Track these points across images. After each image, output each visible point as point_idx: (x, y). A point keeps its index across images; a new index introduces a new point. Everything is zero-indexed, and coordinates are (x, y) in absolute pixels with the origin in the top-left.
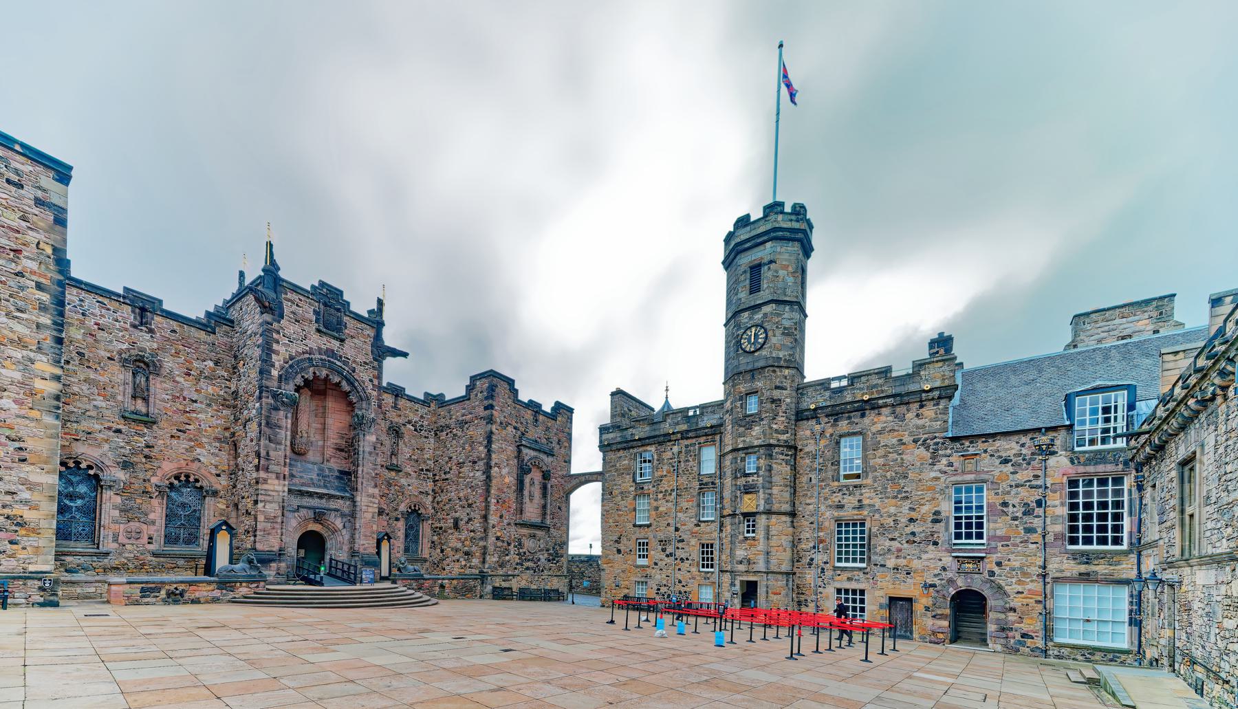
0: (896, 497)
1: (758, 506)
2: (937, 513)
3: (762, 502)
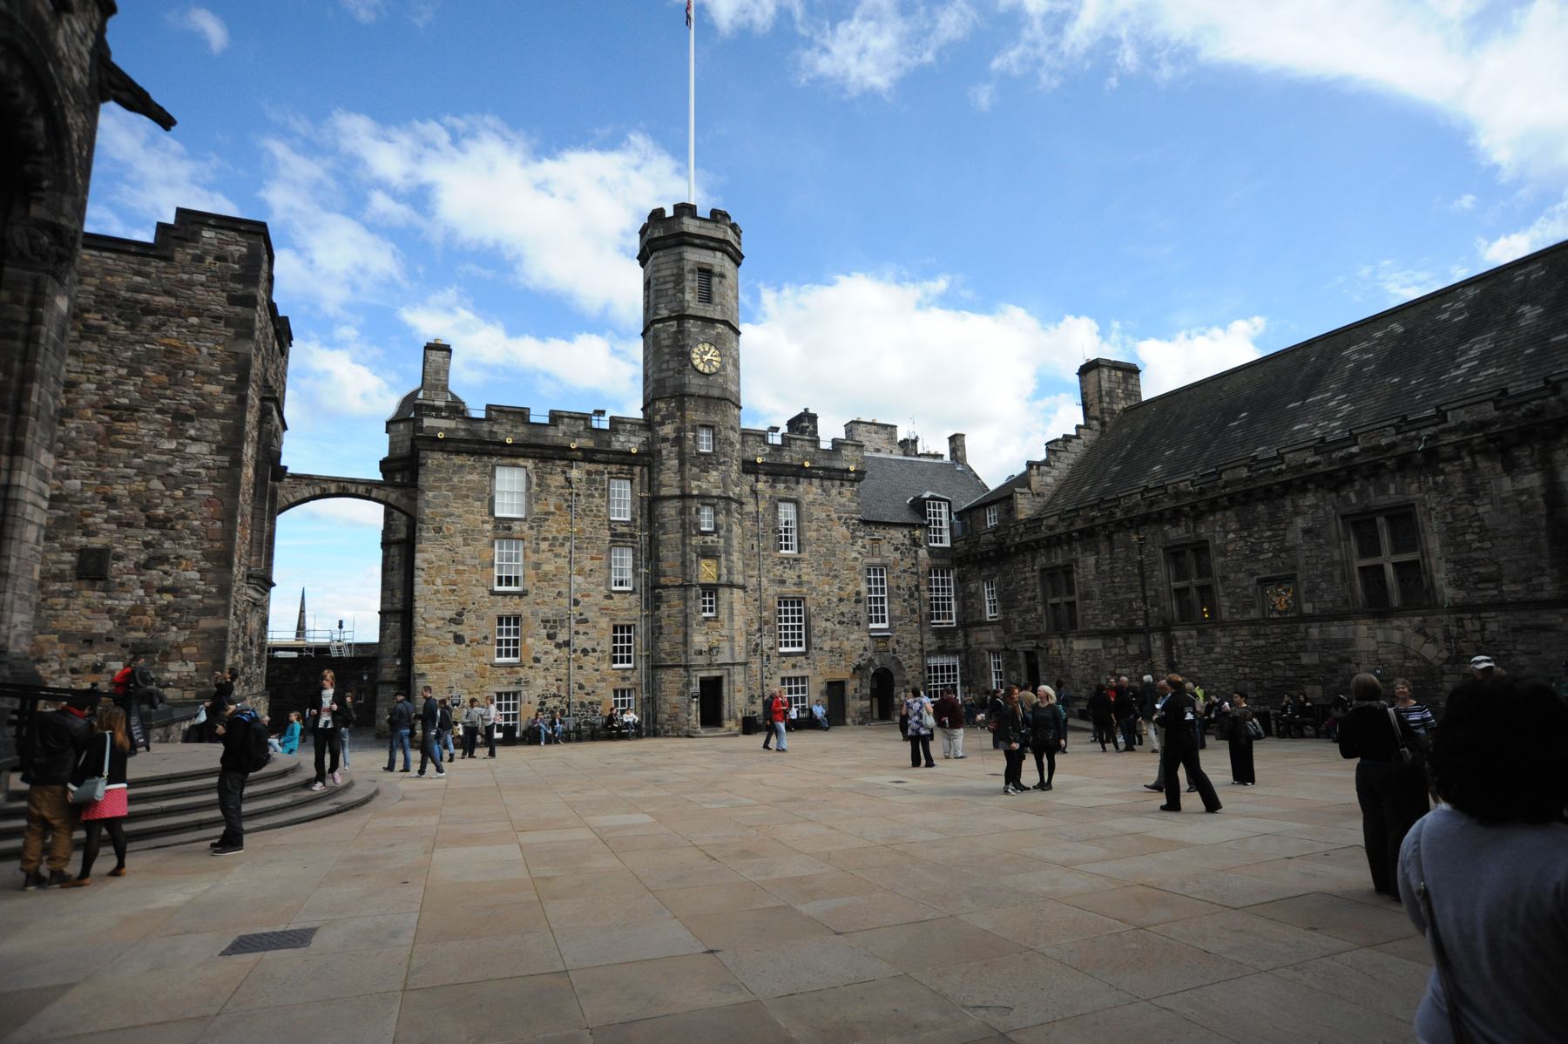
1: (719, 576)
2: (858, 593)
3: (724, 571)
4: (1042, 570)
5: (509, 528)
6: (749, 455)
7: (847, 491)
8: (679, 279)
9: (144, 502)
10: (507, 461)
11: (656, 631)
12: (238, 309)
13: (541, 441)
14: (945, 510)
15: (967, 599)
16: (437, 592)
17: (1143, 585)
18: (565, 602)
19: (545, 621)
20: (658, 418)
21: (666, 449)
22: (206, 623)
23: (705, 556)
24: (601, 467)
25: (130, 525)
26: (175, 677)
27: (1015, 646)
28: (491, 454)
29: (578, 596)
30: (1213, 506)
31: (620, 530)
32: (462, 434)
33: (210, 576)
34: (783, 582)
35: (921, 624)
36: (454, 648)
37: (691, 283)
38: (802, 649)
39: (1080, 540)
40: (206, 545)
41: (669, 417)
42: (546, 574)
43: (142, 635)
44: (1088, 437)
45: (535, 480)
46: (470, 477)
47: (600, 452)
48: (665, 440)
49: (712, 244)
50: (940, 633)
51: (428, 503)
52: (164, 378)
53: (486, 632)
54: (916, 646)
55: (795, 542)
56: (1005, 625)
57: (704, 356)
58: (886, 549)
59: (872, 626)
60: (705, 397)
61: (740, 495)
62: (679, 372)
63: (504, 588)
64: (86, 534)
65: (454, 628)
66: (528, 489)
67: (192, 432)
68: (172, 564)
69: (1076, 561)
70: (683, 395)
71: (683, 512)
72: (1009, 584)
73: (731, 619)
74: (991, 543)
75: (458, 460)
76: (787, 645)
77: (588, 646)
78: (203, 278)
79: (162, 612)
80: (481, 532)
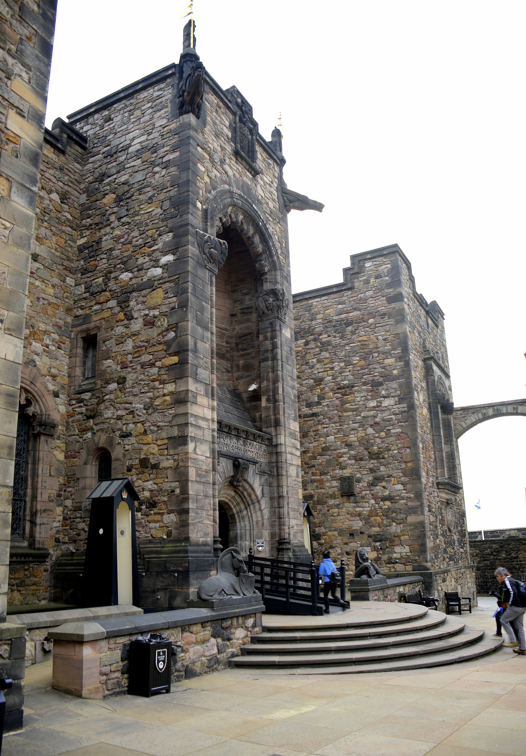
9: (366, 443)
12: (393, 305)
22: (411, 519)
25: (361, 459)
26: (398, 556)
33: (408, 486)
40: (403, 466)
43: (377, 529)
52: (362, 363)
64: (342, 468)
67: (383, 392)
68: (387, 481)
78: (371, 293)
79: (386, 513)
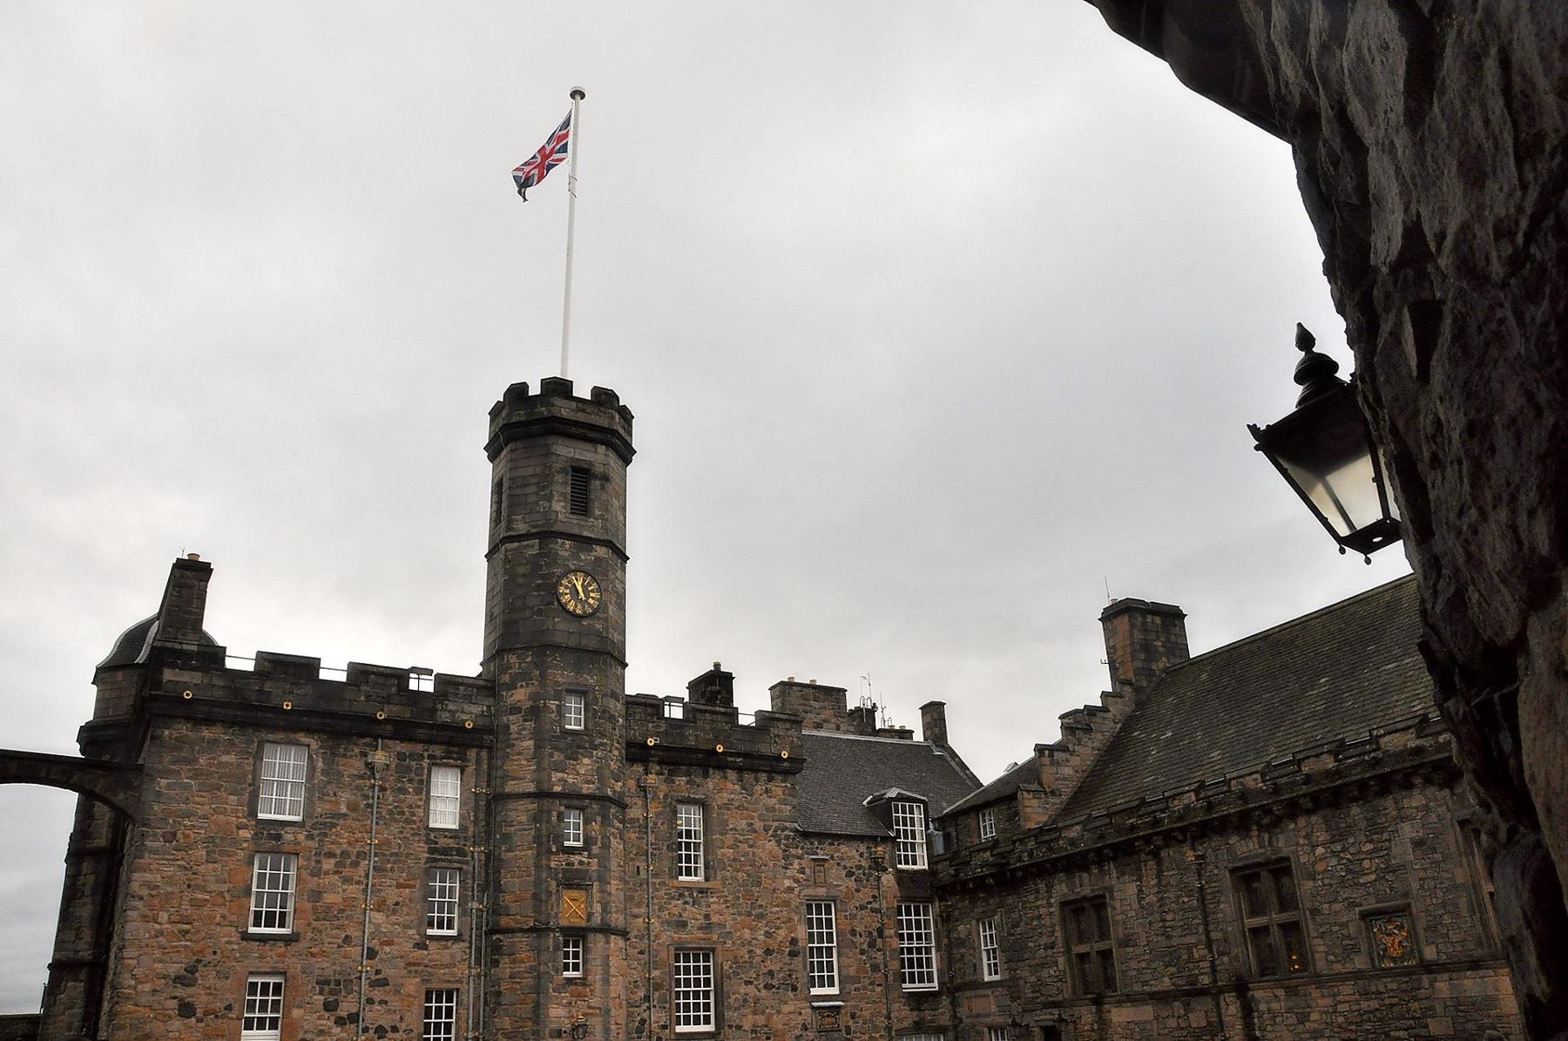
0: (749, 914)
1: (590, 916)
2: (794, 941)
3: (598, 908)
4: (1064, 904)
5: (278, 837)
6: (636, 733)
7: (779, 787)
8: (545, 481)
10: (280, 736)
11: (492, 1000)
13: (334, 707)
14: (918, 815)
15: (955, 949)
16: (160, 933)
17: (1206, 924)
18: (355, 951)
19: (323, 983)
20: (506, 678)
21: (515, 722)
23: (569, 886)
24: (419, 748)
27: (1027, 1020)
28: (258, 726)
29: (375, 943)
30: (1294, 810)
31: (443, 843)
32: (219, 694)
34: (684, 925)
35: (887, 987)
36: (177, 1024)
37: (562, 485)
38: (710, 1028)
39: (1114, 859)
41: (524, 676)
42: (329, 908)
44: (1116, 709)
45: (320, 764)
46: (225, 758)
47: (419, 725)
48: (515, 710)
49: (590, 434)
50: (918, 1000)
51: (159, 794)
53: (230, 998)
54: (881, 1022)
55: (701, 865)
56: (1010, 986)
57: (577, 591)
58: (836, 876)
59: (815, 991)
60: (577, 650)
61: (622, 794)
62: (539, 612)
63: (263, 930)
65: (181, 992)
66: (310, 778)
69: (1110, 889)
70: (546, 646)
71: (536, 819)
72: (1015, 926)
73: (606, 982)
74: (986, 864)
75: (206, 733)
76: (687, 1023)
77: (386, 1022)
80: (236, 842)
